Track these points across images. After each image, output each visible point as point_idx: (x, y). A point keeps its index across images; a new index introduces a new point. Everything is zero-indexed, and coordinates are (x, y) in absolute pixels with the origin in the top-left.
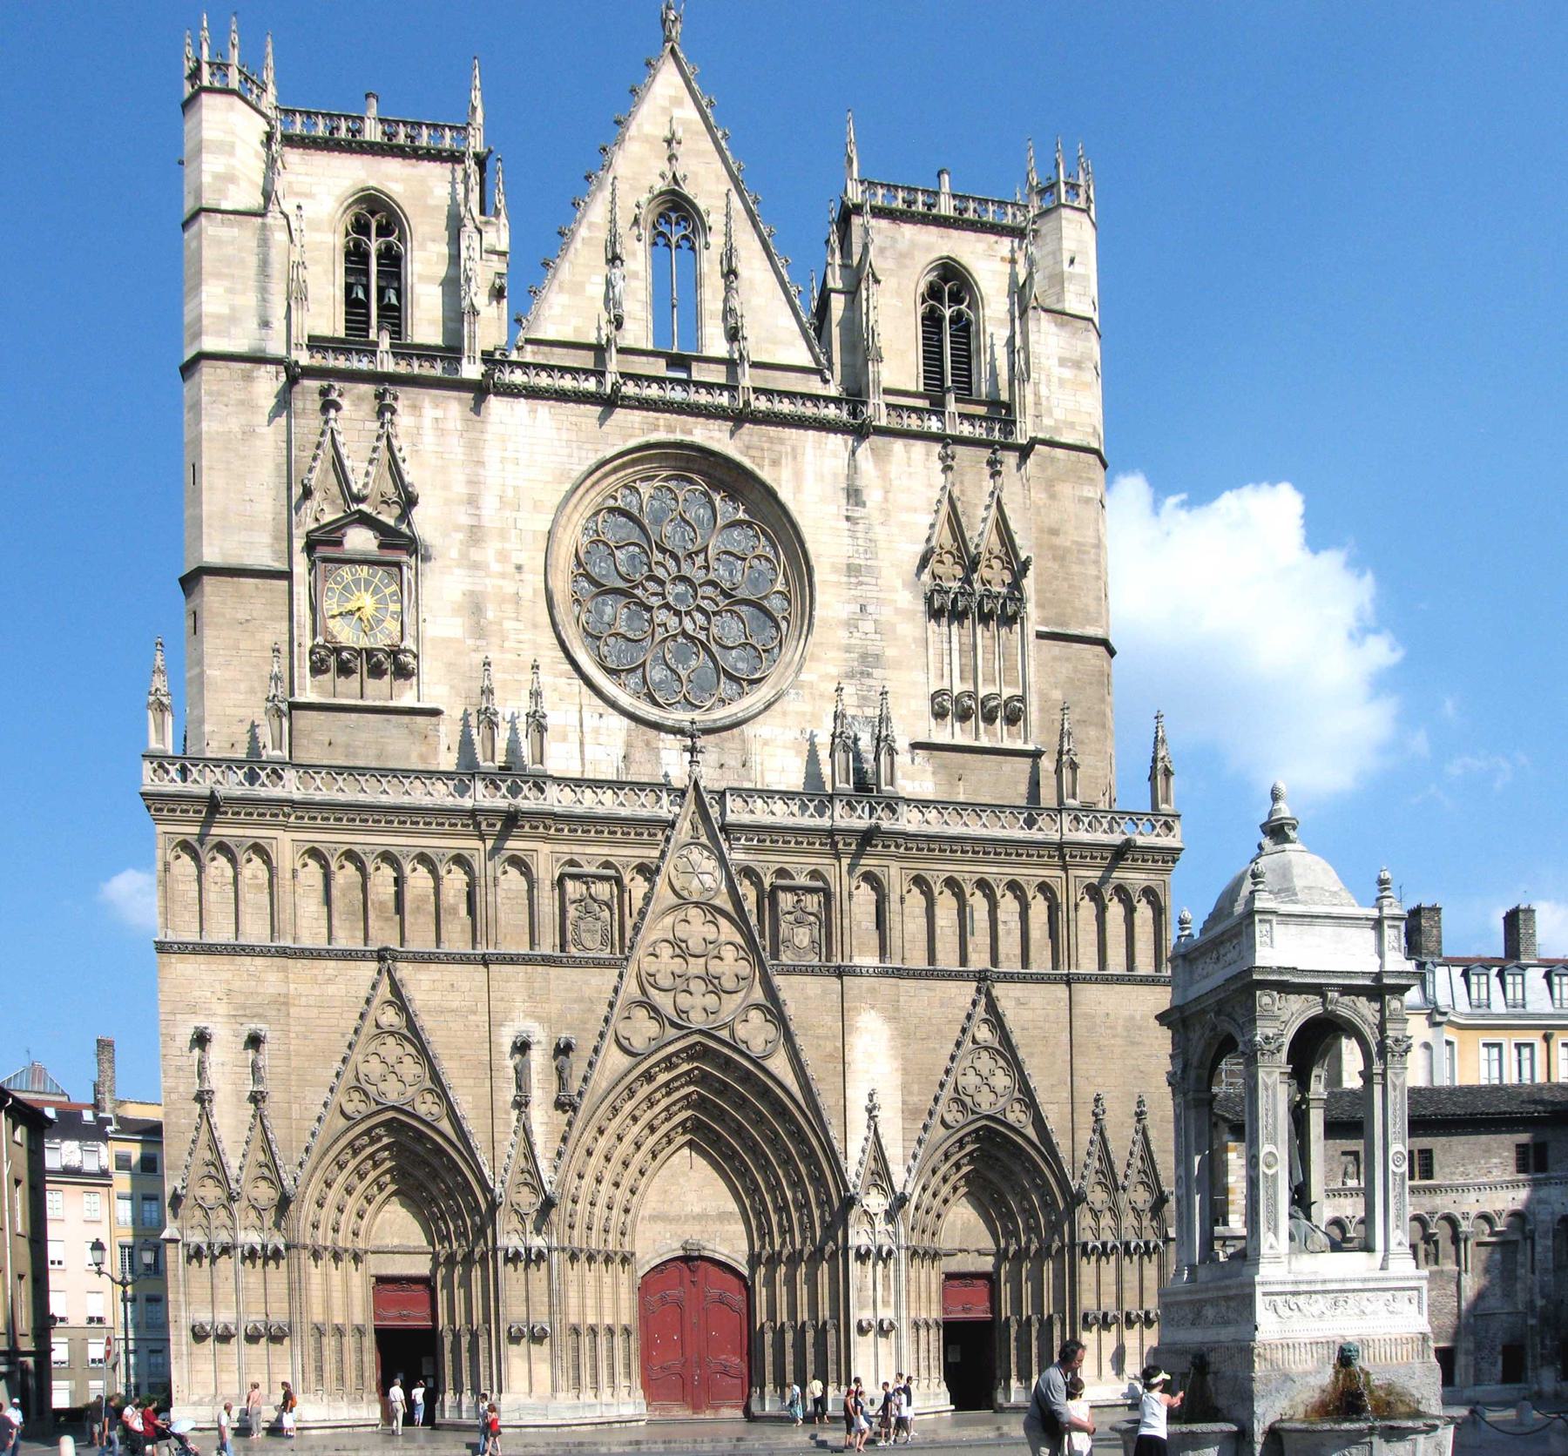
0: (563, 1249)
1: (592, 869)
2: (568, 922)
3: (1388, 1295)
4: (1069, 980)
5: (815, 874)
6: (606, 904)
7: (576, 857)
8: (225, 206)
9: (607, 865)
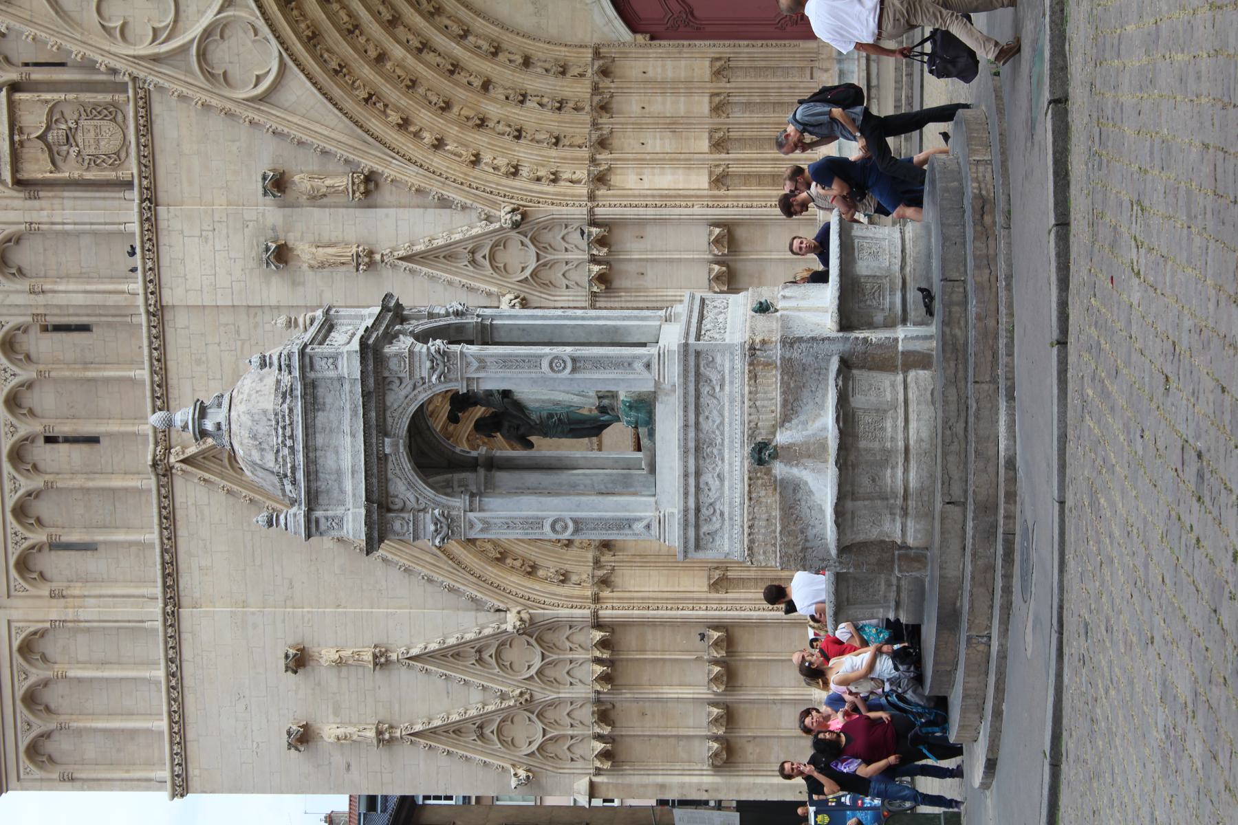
0: (592, 197)
2: (89, 176)
3: (705, 390)
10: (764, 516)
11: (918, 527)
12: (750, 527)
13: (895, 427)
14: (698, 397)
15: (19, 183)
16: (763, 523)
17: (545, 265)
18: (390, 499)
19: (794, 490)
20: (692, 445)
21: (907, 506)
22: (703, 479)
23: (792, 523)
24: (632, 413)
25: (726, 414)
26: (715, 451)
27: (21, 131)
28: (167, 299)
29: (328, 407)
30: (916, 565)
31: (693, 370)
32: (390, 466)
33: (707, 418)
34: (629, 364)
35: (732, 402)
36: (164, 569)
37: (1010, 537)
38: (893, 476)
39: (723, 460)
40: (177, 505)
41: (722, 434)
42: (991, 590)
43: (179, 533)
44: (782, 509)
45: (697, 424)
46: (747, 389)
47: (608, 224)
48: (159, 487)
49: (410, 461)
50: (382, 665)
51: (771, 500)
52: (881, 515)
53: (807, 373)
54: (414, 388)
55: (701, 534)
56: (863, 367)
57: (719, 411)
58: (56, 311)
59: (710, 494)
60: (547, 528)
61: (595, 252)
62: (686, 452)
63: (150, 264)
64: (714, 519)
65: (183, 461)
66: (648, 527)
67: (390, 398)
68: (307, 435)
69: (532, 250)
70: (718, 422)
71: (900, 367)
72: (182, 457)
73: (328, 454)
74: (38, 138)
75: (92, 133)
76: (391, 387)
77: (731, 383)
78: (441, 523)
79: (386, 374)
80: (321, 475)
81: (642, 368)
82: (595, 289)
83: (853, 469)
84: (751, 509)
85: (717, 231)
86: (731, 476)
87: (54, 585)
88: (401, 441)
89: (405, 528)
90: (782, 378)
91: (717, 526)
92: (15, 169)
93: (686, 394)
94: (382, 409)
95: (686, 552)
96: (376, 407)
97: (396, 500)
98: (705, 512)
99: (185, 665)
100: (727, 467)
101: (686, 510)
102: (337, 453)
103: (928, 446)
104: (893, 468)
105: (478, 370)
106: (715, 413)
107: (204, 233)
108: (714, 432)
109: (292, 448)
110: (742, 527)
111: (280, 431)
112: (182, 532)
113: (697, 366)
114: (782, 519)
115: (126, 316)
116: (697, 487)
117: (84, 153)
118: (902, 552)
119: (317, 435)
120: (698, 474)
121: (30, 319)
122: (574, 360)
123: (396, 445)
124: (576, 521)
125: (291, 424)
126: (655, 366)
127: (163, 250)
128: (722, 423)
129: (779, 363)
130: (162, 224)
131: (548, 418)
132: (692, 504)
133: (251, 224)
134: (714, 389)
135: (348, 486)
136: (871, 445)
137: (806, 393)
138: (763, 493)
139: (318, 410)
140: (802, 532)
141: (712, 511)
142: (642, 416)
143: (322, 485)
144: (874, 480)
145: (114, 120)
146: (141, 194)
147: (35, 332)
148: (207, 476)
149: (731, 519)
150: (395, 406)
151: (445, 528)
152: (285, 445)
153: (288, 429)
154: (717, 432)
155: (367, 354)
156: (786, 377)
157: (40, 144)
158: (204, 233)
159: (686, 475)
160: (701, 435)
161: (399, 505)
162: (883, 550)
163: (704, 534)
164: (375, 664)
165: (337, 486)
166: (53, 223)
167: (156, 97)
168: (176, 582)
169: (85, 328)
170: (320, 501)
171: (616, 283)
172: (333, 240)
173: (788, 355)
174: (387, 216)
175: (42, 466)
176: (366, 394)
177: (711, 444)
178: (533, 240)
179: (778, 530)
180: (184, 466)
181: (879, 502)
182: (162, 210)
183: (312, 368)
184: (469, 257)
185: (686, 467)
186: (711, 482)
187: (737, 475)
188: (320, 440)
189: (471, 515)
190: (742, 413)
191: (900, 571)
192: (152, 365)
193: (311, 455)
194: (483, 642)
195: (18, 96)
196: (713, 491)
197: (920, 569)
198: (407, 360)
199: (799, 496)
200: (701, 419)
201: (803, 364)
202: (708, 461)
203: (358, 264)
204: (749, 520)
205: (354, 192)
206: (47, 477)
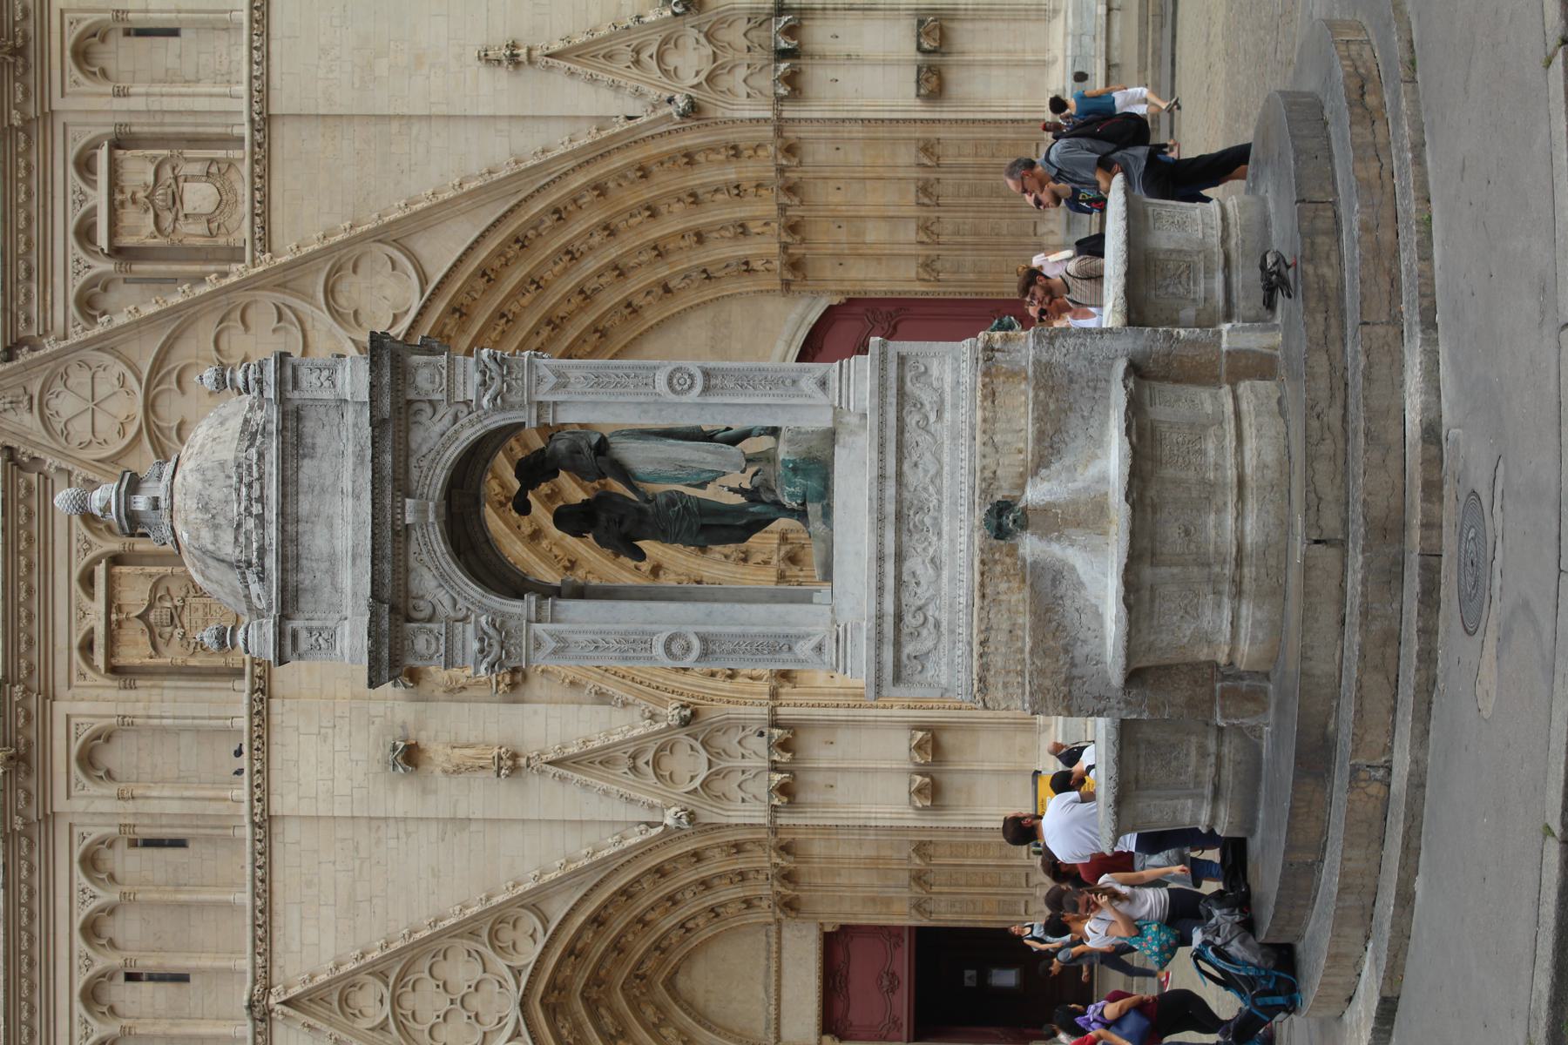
0: (774, 695)
1: (99, 605)
2: (193, 662)
3: (912, 420)
5: (85, 165)
6: (155, 587)
7: (76, 641)
9: (87, 580)
10: (1005, 626)
11: (1259, 615)
12: (981, 643)
13: (1221, 449)
14: (901, 430)
15: (114, 670)
16: (1003, 637)
17: (717, 773)
18: (412, 602)
19: (1054, 580)
20: (890, 508)
21: (1241, 577)
22: (908, 565)
23: (1049, 636)
24: (799, 480)
25: (946, 459)
26: (928, 521)
27: (119, 609)
28: (276, 807)
29: (319, 451)
30: (1250, 706)
31: (894, 386)
32: (413, 547)
33: (916, 465)
34: (794, 382)
35: (955, 437)
37: (1433, 560)
38: (1219, 525)
39: (939, 534)
41: (939, 492)
42: (1393, 677)
44: (1034, 613)
45: (900, 475)
46: (979, 414)
47: (793, 727)
48: (255, 1034)
49: (445, 543)
51: (1016, 597)
52: (1197, 595)
53: (1076, 386)
54: (456, 419)
55: (904, 658)
56: (1165, 378)
57: (934, 454)
58: (146, 821)
59: (919, 591)
60: (659, 650)
61: (776, 758)
62: (881, 520)
63: (258, 766)
64: (925, 632)
65: (284, 1003)
66: (819, 648)
67: (417, 436)
68: (284, 496)
69: (704, 755)
70: (932, 472)
71: (1224, 377)
72: (284, 998)
73: (318, 528)
74: (138, 617)
75: (200, 613)
76: (418, 418)
77: (955, 406)
78: (490, 638)
79: (412, 395)
80: (304, 562)
81: (814, 387)
82: (776, 802)
83: (1154, 512)
84: (984, 614)
85: (920, 735)
88: (431, 504)
89: (433, 647)
90: (1036, 396)
91: (929, 644)
92: (110, 653)
93: (882, 425)
94: (404, 454)
95: (878, 686)
96: (394, 448)
97: (422, 603)
98: (908, 618)
100: (945, 546)
101: (880, 617)
102: (331, 526)
103: (1277, 475)
104: (1219, 511)
105: (555, 388)
106: (928, 455)
107: (323, 731)
108: (925, 489)
109: (260, 518)
110: (970, 644)
111: (244, 490)
113: (901, 381)
114: (1033, 629)
115: (228, 828)
117: (189, 635)
118: (1228, 683)
119: (301, 497)
120: (900, 558)
121: (116, 830)
122: (707, 374)
123: (423, 512)
124: (704, 639)
125: (261, 478)
127: (275, 749)
128: (939, 474)
129: (1030, 372)
130: (276, 719)
131: (667, 505)
132: (889, 606)
133: (377, 721)
134: (926, 418)
135: (346, 579)
136: (1183, 475)
137: (1074, 421)
138: (1003, 586)
139: (304, 456)
140: (1066, 651)
141: (921, 620)
142: (814, 484)
143: (306, 579)
144: (1187, 533)
146: (253, 683)
147: (121, 846)
148: (312, 1021)
149: (952, 632)
150: (424, 450)
151: (496, 648)
152: (250, 514)
153: (256, 486)
155: (381, 356)
156: (1042, 394)
157: (141, 625)
158: (323, 731)
159: (881, 559)
160: (906, 494)
161: (427, 612)
162: (1196, 682)
165: (328, 581)
166: (149, 717)
169: (179, 843)
170: (302, 605)
171: (802, 797)
172: (472, 740)
173: (1045, 357)
174: (535, 712)
175: (120, 1008)
176: (377, 424)
177: (921, 509)
178: (704, 744)
179: (1027, 649)
180: (286, 1009)
181: (1196, 569)
182: (276, 704)
183: (296, 385)
184: (629, 762)
185: (881, 544)
186: (920, 571)
187: (962, 557)
188: (305, 505)
189: (537, 627)
190: (972, 455)
191: (1224, 716)
192: (254, 886)
193: (289, 528)
195: (117, 569)
197: (1256, 713)
198: (444, 372)
199: (1061, 590)
200: (906, 467)
201: (1070, 372)
202: (916, 536)
203: (500, 768)
204: (981, 632)
205: (498, 683)
206: (125, 1022)
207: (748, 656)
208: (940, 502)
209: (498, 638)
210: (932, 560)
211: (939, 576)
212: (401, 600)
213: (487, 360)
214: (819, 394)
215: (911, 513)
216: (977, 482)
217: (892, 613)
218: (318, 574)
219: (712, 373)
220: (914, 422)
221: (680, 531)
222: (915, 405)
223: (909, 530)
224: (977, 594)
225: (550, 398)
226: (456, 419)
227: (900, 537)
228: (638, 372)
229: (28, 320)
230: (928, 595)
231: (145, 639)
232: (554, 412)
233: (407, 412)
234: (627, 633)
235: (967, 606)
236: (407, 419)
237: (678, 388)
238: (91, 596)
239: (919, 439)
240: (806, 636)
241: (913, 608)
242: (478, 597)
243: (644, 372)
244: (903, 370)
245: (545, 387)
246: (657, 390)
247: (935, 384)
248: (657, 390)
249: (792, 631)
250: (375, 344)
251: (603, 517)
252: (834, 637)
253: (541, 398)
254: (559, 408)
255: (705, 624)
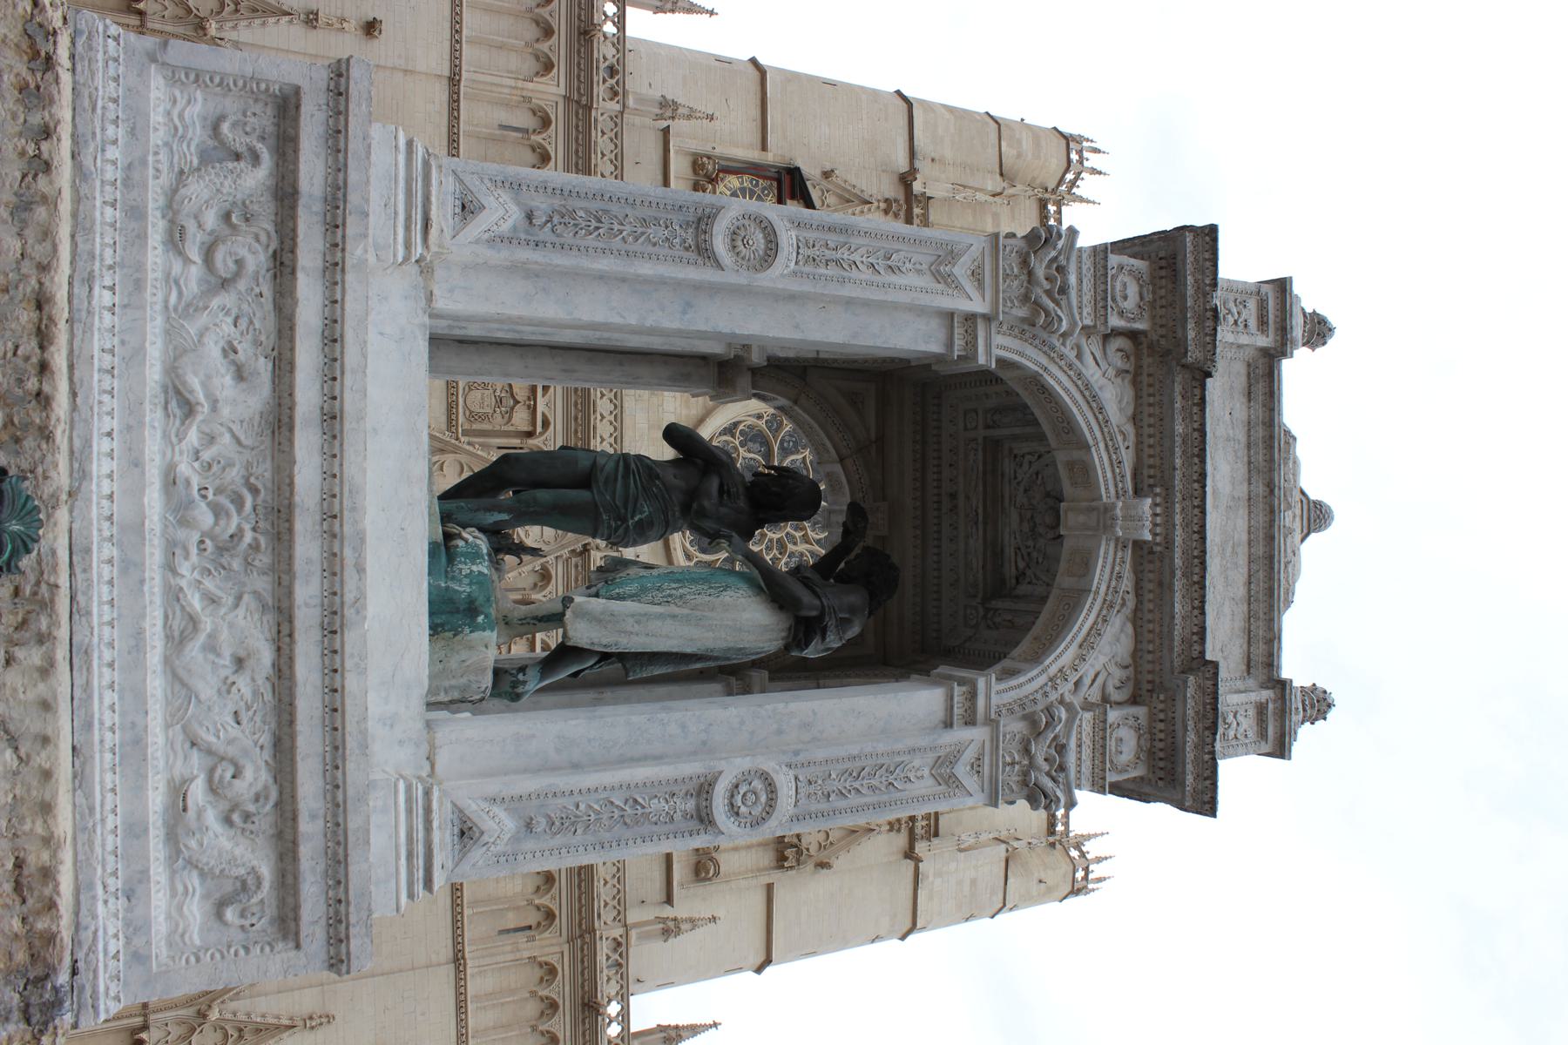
1: (540, 408)
3: (256, 776)
4: (458, 960)
6: (510, 418)
8: (1003, 143)
9: (546, 424)
20: (307, 548)
22: (257, 399)
24: (463, 589)
25: (156, 684)
26: (205, 518)
27: (529, 407)
33: (239, 663)
34: (529, 825)
35: (136, 744)
36: (458, 106)
39: (171, 480)
40: (446, 148)
41: (174, 595)
43: (446, 129)
46: (64, 823)
50: (312, 13)
57: (190, 694)
60: (788, 238)
62: (331, 517)
64: (211, 219)
66: (467, 209)
67: (1124, 647)
70: (194, 650)
74: (519, 402)
77: (135, 830)
80: (1242, 437)
81: (487, 824)
84: (39, 251)
86: (134, 409)
87: (528, 105)
98: (257, 260)
99: (449, 37)
100: (153, 449)
101: (334, 269)
106: (207, 689)
108: (212, 601)
112: (444, 130)
116: (283, 366)
117: (491, 391)
119: (1245, 537)
120: (279, 422)
126: (443, 837)
128: (177, 641)
134: (213, 789)
141: (219, 255)
145: (471, 412)
149: (136, 213)
154: (196, 602)
157: (518, 398)
159: (331, 419)
160: (263, 584)
163: (256, 159)
164: (317, 14)
167: (444, 426)
168: (450, 96)
177: (221, 550)
183: (1261, 709)
187: (105, 421)
189: (978, 305)
190: (81, 701)
193: (1261, 489)
194: (234, 17)
195: (530, 429)
196: (213, 350)
198: (1108, 765)
200: (266, 656)
202: (235, 475)
204: (49, 201)
207: (615, 208)
208: (170, 568)
209: (1039, 291)
210: (189, 409)
211: (172, 371)
212: (1145, 371)
213: (1059, 794)
214: (473, 808)
215: (248, 537)
216: (63, 633)
217: (300, 275)
218: (1227, 417)
219: (694, 824)
220: (249, 773)
221: (626, 476)
222: (247, 817)
223: (255, 491)
224: (61, 310)
225: (961, 734)
226: (1077, 684)
227: (277, 470)
228: (824, 806)
229: (576, 566)
230: (204, 318)
231: (515, 390)
232: (950, 709)
233: (1137, 683)
234: (842, 281)
235: (89, 281)
236: (1137, 672)
237: (758, 784)
238: (544, 414)
239: (234, 731)
240: (497, 240)
241: (242, 285)
242: (1054, 369)
243: (814, 807)
244: (282, 902)
245: (969, 755)
246: (791, 773)
247: (194, 880)
248: (791, 773)
249: (525, 254)
250: (1207, 798)
251: (742, 503)
252: (434, 232)
253: (979, 734)
254: (940, 714)
255: (698, 287)
